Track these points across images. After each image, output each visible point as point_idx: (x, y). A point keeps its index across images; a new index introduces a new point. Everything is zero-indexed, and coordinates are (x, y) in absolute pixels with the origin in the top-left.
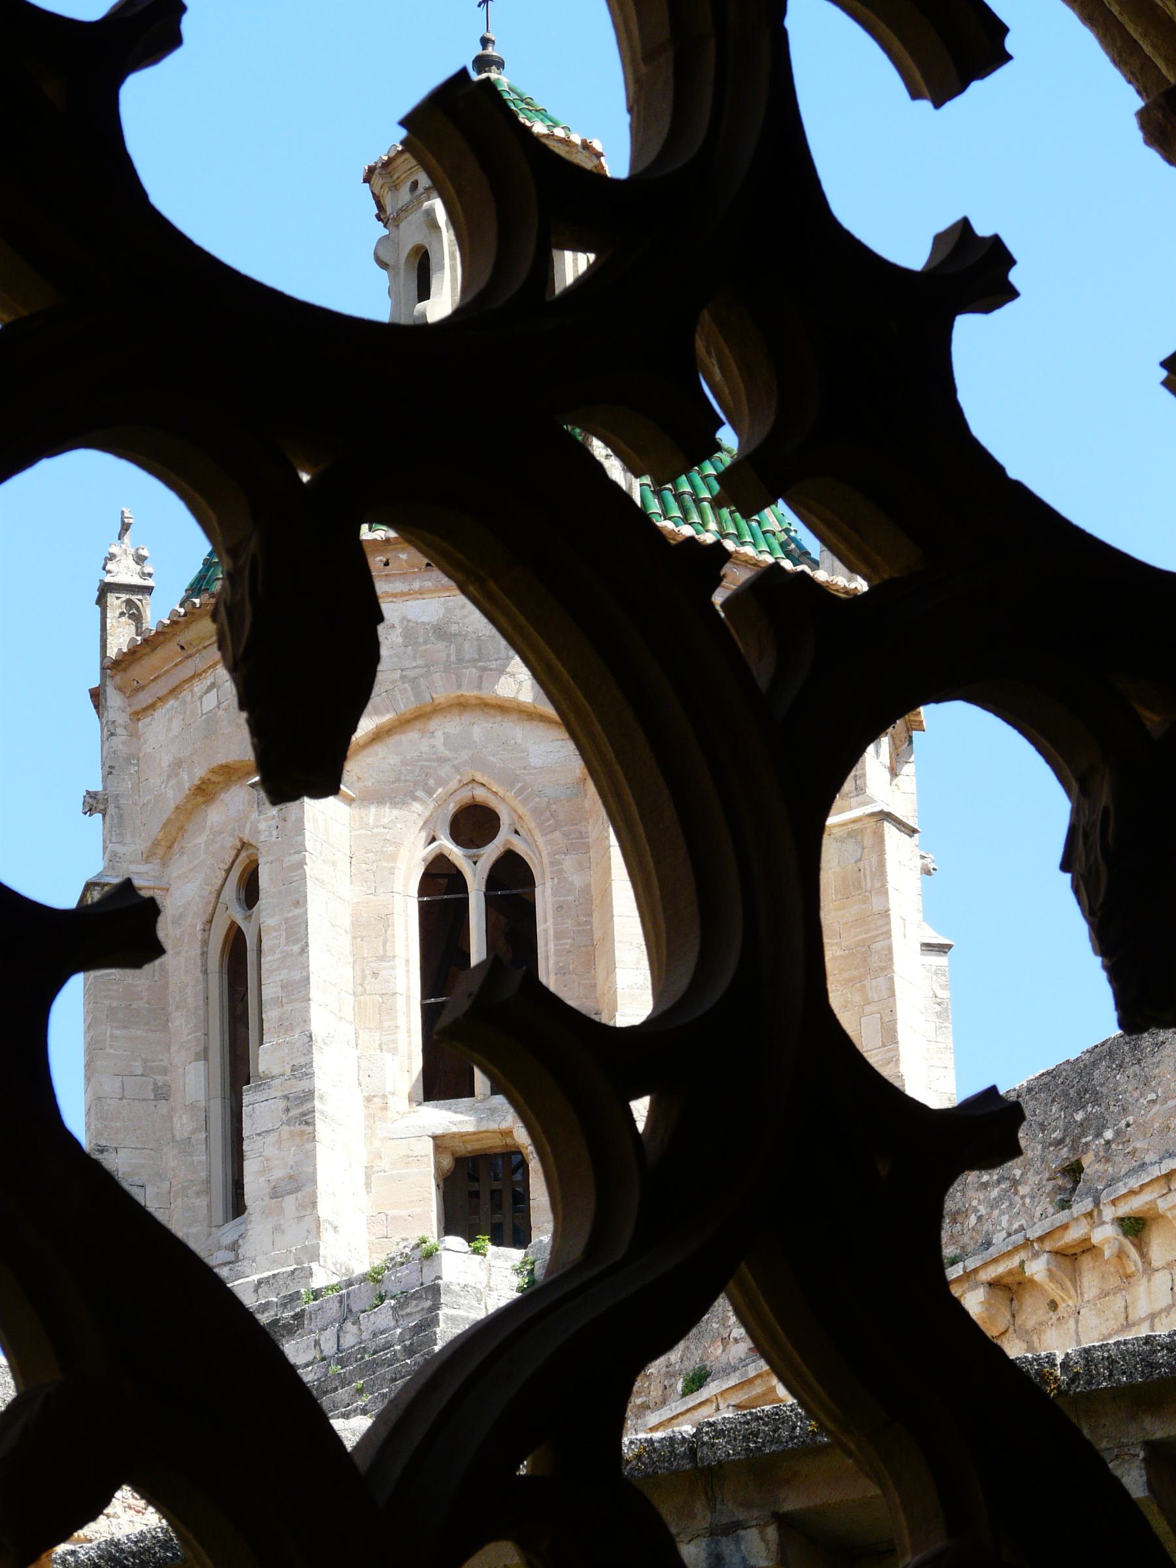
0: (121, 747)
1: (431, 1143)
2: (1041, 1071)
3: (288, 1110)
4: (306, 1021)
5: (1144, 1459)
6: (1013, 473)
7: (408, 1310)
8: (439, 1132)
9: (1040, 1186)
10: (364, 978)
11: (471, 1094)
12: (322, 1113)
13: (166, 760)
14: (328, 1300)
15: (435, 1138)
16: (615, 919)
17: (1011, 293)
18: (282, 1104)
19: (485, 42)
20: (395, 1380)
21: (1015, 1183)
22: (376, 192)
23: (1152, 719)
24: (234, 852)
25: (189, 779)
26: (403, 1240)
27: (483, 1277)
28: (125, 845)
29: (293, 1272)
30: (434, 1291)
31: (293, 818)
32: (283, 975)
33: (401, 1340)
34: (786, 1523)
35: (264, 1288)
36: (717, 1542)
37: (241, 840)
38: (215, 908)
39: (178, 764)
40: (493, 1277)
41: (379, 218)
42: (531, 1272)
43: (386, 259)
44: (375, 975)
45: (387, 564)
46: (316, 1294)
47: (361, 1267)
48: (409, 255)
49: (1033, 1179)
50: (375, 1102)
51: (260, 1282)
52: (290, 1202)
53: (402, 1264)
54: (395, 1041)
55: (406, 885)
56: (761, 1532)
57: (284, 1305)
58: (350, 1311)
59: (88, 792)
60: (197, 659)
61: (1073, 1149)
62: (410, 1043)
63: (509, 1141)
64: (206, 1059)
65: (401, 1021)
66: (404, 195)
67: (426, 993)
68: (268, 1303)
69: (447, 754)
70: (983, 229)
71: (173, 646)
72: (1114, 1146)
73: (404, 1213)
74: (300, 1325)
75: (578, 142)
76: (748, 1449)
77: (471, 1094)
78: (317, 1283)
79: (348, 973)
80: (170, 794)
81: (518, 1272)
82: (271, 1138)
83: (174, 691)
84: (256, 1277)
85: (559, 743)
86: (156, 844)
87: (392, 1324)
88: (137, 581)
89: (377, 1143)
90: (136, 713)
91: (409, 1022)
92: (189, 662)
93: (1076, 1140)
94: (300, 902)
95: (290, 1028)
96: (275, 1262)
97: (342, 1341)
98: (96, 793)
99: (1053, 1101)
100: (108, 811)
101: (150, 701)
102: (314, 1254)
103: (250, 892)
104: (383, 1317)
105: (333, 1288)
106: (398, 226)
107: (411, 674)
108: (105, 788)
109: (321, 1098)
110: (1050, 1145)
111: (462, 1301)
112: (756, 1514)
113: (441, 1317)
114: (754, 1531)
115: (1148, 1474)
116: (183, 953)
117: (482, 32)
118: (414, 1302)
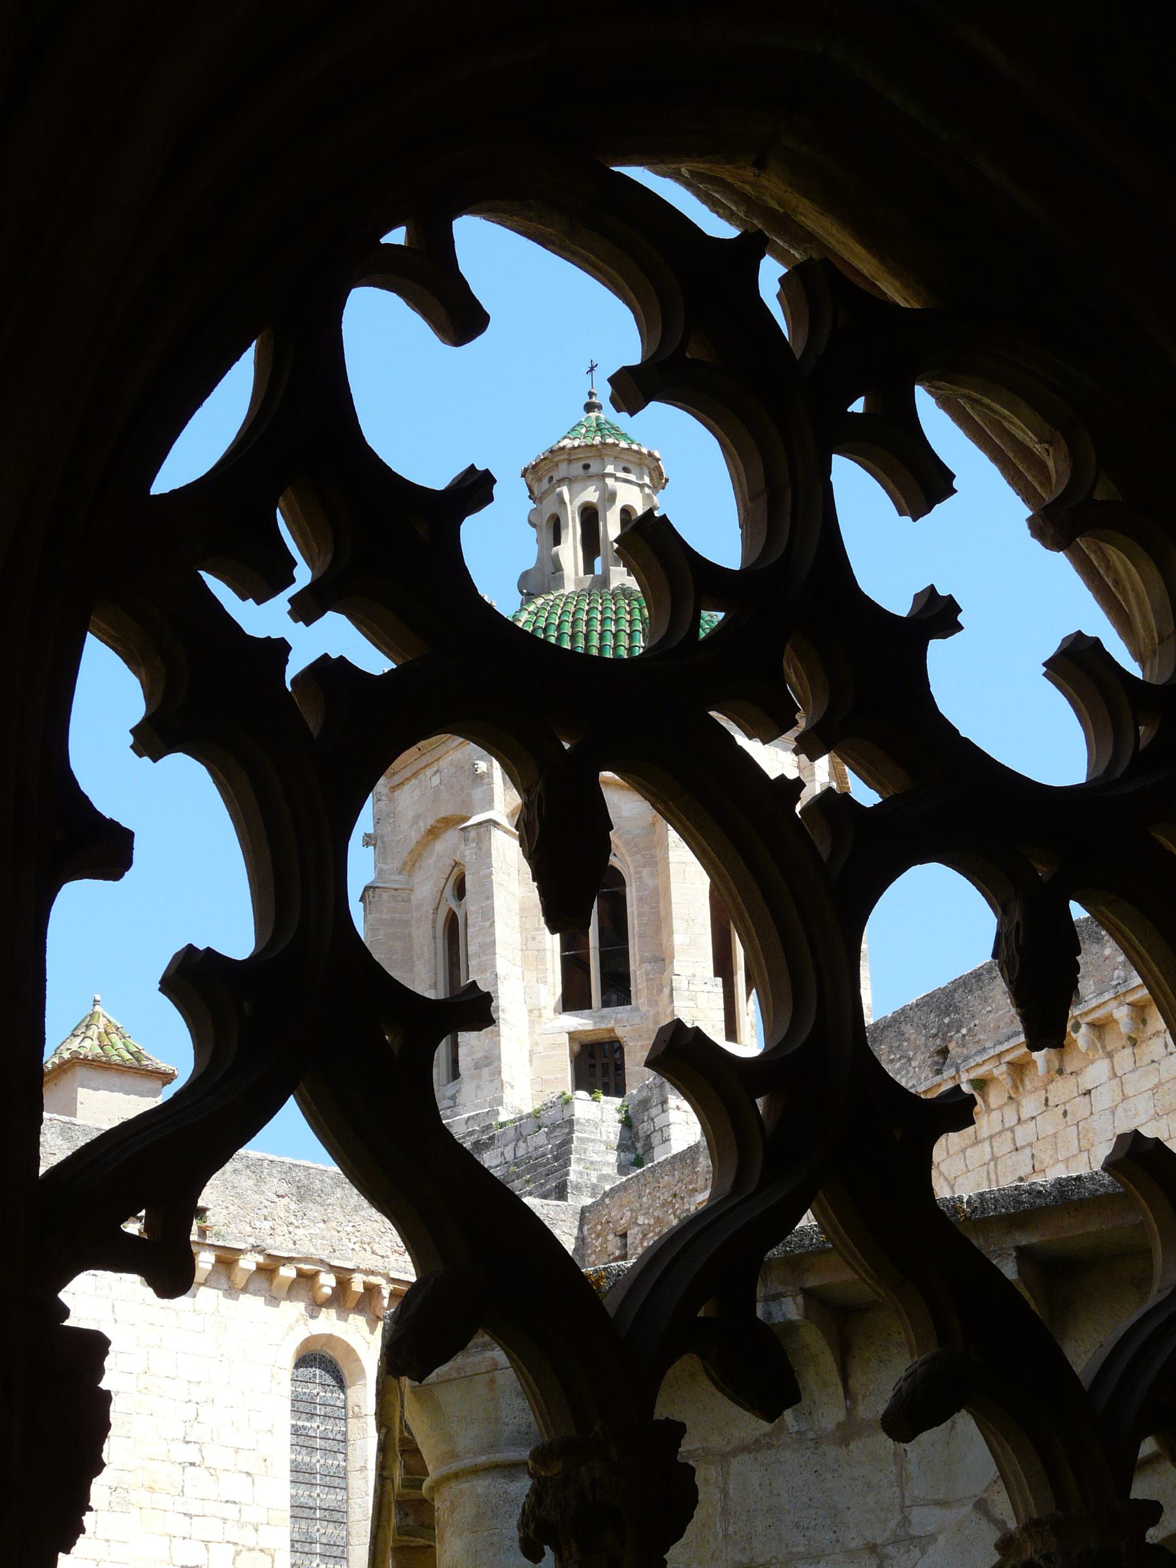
0: (384, 807)
1: (567, 1036)
2: (925, 994)
4: (494, 966)
5: (1016, 1257)
6: (963, 733)
7: (555, 1134)
8: (572, 1030)
9: (924, 1061)
10: (527, 941)
11: (590, 1007)
12: (503, 1019)
13: (410, 814)
14: (508, 1129)
15: (569, 1033)
16: (673, 905)
17: (959, 627)
19: (591, 394)
20: (548, 1175)
21: (910, 1060)
22: (529, 483)
23: (1042, 872)
26: (552, 1093)
27: (599, 1114)
28: (387, 864)
29: (488, 1112)
30: (570, 1123)
31: (485, 848)
32: (480, 939)
33: (551, 1152)
34: (808, 1294)
35: (471, 1122)
36: (768, 1306)
37: (454, 861)
38: (440, 900)
39: (417, 818)
40: (604, 1114)
41: (530, 497)
42: (626, 1111)
43: (534, 521)
44: (534, 939)
46: (502, 1125)
47: (528, 1109)
48: (548, 521)
49: (920, 1057)
50: (535, 1013)
51: (469, 1118)
52: (485, 1072)
53: (551, 1107)
54: (545, 977)
56: (794, 1300)
57: (483, 1132)
58: (521, 1135)
59: (365, 834)
61: (944, 1039)
62: (554, 978)
63: (612, 1035)
64: (436, 988)
65: (549, 965)
66: (545, 484)
68: (473, 1130)
70: (942, 592)
72: (967, 1038)
73: (552, 1077)
74: (493, 1144)
75: (646, 452)
76: (786, 1251)
77: (590, 1007)
78: (502, 1118)
79: (518, 938)
80: (413, 834)
81: (619, 1111)
83: (415, 775)
84: (466, 1116)
86: (405, 864)
87: (546, 1142)
89: (536, 1037)
90: (393, 788)
91: (553, 966)
93: (945, 1035)
94: (490, 897)
95: (484, 971)
96: (477, 1107)
97: (517, 1152)
98: (370, 834)
99: (931, 1011)
100: (377, 844)
101: (401, 781)
102: (500, 1101)
103: (460, 891)
104: (540, 1138)
105: (512, 1121)
106: (541, 502)
108: (375, 831)
109: (503, 1011)
110: (930, 1037)
111: (586, 1128)
112: (791, 1288)
113: (574, 1138)
114: (790, 1298)
115: (1018, 1266)
117: (589, 389)
118: (559, 1130)
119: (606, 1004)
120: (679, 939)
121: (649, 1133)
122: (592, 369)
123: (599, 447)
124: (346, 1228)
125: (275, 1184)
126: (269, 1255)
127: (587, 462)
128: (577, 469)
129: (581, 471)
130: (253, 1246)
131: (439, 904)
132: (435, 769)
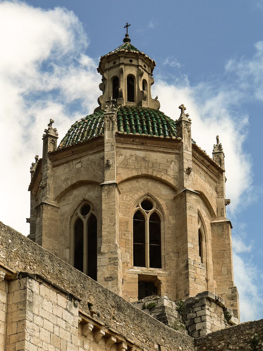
0: (50, 173)
3: (110, 261)
15: (139, 275)
16: (188, 231)
18: (108, 260)
24: (81, 202)
25: (70, 183)
37: (84, 199)
39: (66, 179)
44: (125, 235)
45: (133, 141)
55: (131, 216)
60: (76, 155)
67: (135, 241)
69: (143, 187)
71: (70, 151)
82: (105, 267)
83: (67, 162)
85: (168, 190)
88: (54, 135)
92: (73, 156)
107: (137, 167)
116: (64, 223)
119: (151, 266)
120: (190, 245)
121: (193, 317)
122: (127, 26)
123: (138, 54)
124: (131, 326)
125: (111, 302)
126: (110, 330)
127: (132, 59)
128: (127, 61)
129: (129, 63)
130: (106, 325)
131: (73, 215)
132: (78, 161)
